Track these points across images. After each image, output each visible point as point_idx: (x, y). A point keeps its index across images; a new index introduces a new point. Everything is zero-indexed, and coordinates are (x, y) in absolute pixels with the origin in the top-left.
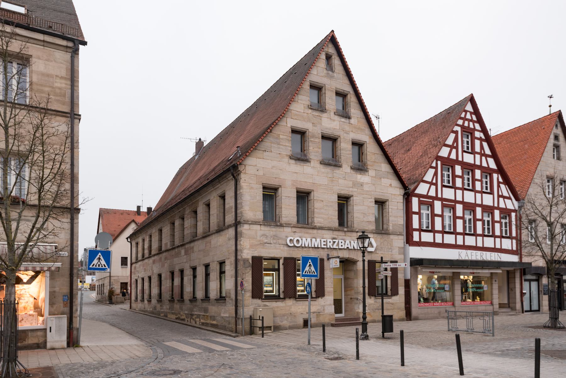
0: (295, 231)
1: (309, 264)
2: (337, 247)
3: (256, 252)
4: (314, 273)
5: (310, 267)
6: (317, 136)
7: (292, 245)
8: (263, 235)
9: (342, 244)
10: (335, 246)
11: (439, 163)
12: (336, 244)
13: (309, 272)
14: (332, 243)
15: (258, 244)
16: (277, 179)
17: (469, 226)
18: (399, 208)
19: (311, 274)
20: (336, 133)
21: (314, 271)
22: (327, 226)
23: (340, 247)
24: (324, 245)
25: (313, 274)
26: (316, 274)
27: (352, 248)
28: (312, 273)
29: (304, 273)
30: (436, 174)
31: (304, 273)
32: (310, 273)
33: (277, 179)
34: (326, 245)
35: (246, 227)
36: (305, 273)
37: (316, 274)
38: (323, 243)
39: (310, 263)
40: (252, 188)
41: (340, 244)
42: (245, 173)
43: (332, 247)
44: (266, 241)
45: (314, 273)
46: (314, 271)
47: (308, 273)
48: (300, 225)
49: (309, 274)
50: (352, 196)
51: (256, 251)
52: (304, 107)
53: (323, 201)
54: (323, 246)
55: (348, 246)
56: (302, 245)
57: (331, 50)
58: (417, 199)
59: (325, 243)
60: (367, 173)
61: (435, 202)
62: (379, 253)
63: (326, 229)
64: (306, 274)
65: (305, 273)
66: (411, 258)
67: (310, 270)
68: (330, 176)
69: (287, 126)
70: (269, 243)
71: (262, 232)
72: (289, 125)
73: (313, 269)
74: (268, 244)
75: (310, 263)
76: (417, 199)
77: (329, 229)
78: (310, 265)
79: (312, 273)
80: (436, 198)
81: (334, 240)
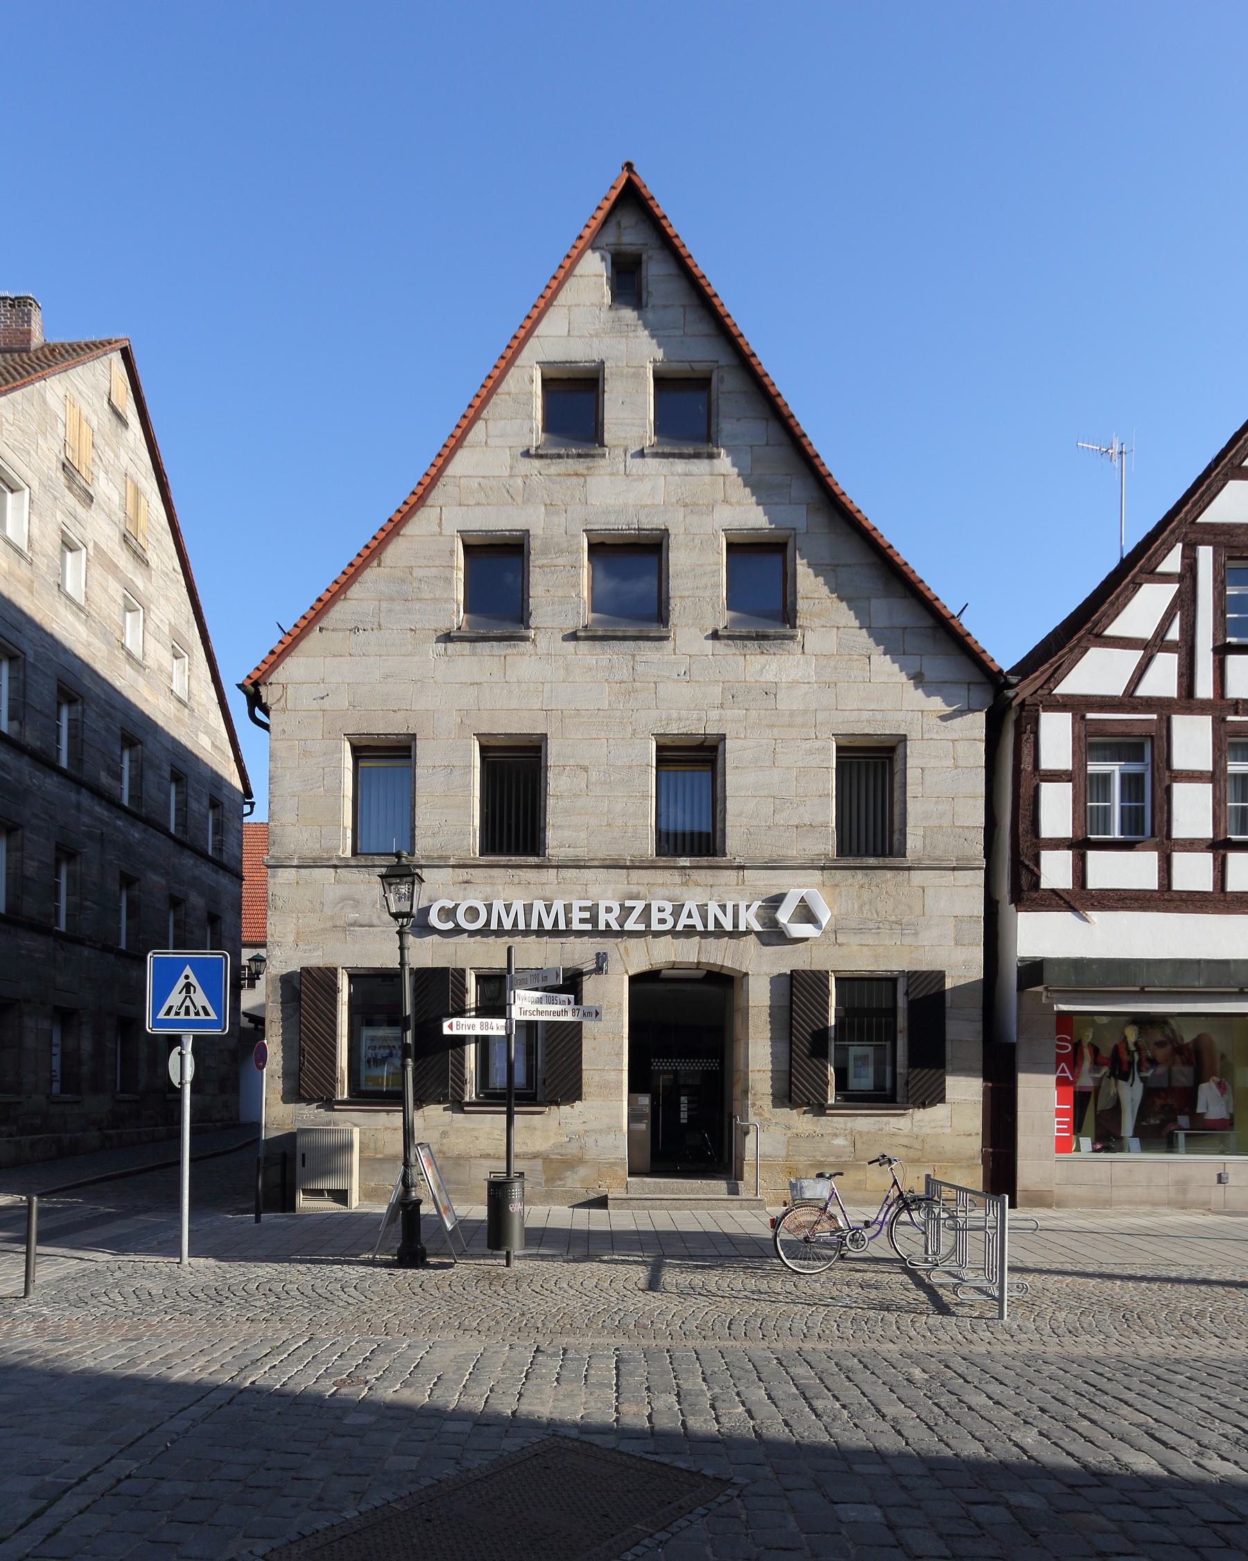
0: (466, 877)
1: (182, 982)
2: (642, 927)
3: (316, 954)
4: (207, 1014)
5: (188, 992)
6: (565, 545)
7: (450, 925)
8: (343, 899)
9: (662, 915)
10: (630, 925)
11: (1205, 554)
12: (635, 914)
13: (183, 1010)
14: (617, 911)
15: (324, 930)
16: (399, 713)
17: (1143, 801)
18: (961, 763)
19: (192, 1016)
20: (651, 522)
21: (204, 1008)
22: (600, 855)
23: (655, 926)
24: (582, 921)
25: (203, 1016)
26: (213, 1016)
27: (711, 927)
28: (197, 1014)
29: (161, 1016)
30: (1185, 603)
31: (161, 1016)
32: (187, 1013)
33: (400, 715)
34: (594, 920)
35: (285, 875)
36: (168, 1013)
37: (213, 1016)
38: (576, 915)
39: (187, 977)
40: (306, 753)
41: (655, 916)
42: (284, 710)
43: (616, 927)
44: (353, 916)
45: (207, 1014)
46: (204, 1008)
47: (177, 1014)
48: (852, 861)
49: (182, 1016)
50: (723, 738)
51: (316, 949)
52: (512, 457)
53: (585, 769)
54: (576, 926)
55: (690, 922)
56: (488, 923)
57: (632, 236)
58: (1066, 718)
59: (587, 915)
60: (794, 646)
61: (1178, 721)
62: (847, 944)
63: (596, 863)
64: (172, 1016)
65: (168, 1013)
66: (1022, 960)
67: (188, 1003)
68: (618, 678)
69: (441, 534)
70: (366, 922)
71: (341, 890)
72: (451, 528)
73: (200, 998)
74: (361, 926)
75: (187, 977)
76: (1066, 718)
77: (608, 863)
78: (188, 986)
79: (197, 1014)
80: (1187, 700)
81: (628, 903)
